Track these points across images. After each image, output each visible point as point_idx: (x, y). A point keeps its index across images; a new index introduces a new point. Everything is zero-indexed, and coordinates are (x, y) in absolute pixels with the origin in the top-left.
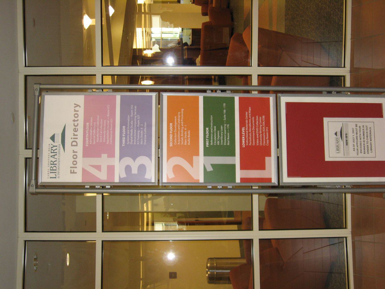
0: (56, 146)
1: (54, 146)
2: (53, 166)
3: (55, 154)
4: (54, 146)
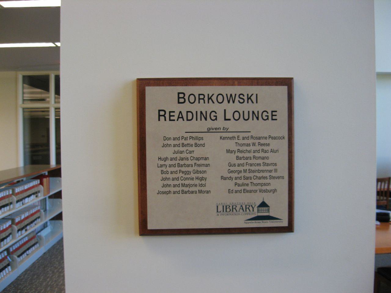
0: (253, 211)
1: (253, 208)
2: (231, 208)
3: (245, 210)
4: (253, 208)
